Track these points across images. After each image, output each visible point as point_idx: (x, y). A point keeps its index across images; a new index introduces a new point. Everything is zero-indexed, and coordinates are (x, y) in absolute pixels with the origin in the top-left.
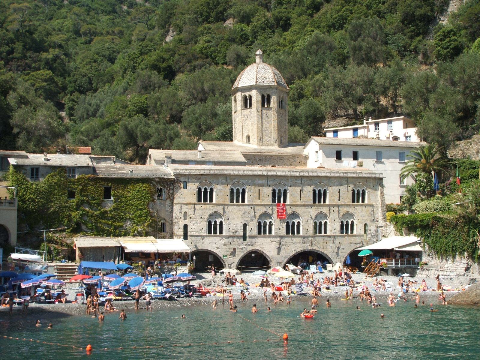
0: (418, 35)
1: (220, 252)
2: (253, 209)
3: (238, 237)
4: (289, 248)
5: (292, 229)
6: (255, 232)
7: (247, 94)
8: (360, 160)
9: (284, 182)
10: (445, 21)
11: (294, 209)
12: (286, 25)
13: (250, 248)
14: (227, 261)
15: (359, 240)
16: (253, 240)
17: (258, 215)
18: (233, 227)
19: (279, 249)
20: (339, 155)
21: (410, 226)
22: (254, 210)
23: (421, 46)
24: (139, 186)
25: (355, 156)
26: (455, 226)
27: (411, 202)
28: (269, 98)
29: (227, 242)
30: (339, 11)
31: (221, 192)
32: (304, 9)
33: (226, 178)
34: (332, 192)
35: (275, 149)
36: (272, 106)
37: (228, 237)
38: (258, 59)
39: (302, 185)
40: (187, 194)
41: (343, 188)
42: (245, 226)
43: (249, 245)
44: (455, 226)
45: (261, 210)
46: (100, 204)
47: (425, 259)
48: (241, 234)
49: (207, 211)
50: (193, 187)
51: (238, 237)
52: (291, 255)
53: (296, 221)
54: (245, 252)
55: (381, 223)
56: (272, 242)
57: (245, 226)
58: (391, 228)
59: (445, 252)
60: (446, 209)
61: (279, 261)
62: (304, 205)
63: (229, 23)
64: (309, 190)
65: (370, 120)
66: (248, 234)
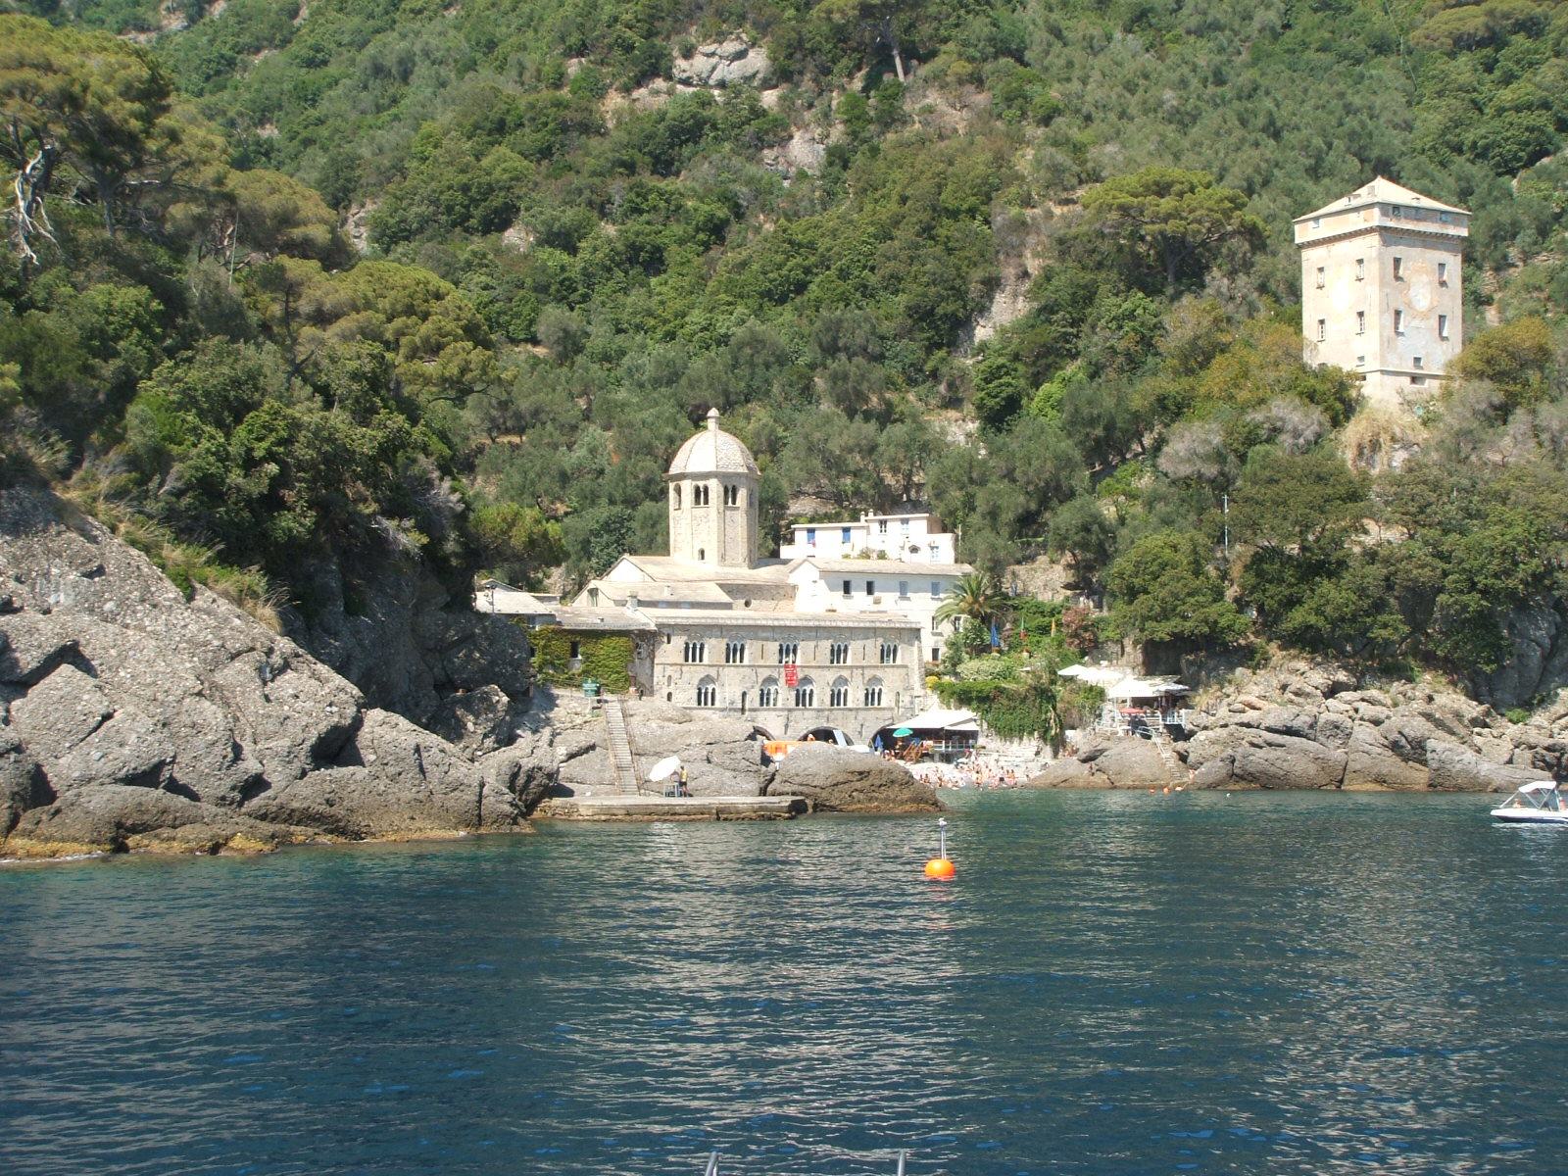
0: (939, 346)
5: (801, 699)
6: (757, 704)
7: (701, 484)
8: (877, 594)
10: (982, 332)
11: (807, 672)
12: (655, 262)
15: (888, 714)
20: (847, 588)
21: (964, 698)
23: (944, 370)
24: (615, 641)
25: (870, 589)
26: (1024, 700)
27: (955, 662)
28: (735, 491)
30: (780, 267)
31: (714, 649)
32: (690, 229)
33: (721, 630)
34: (855, 647)
35: (743, 573)
36: (739, 503)
38: (711, 424)
39: (817, 638)
40: (670, 652)
41: (869, 643)
42: (744, 694)
44: (1024, 700)
45: (765, 673)
46: (565, 666)
47: (981, 741)
50: (679, 642)
53: (808, 689)
55: (918, 690)
57: (744, 694)
58: (934, 699)
59: (1009, 731)
60: (1008, 673)
63: (515, 237)
64: (826, 645)
65: (871, 515)
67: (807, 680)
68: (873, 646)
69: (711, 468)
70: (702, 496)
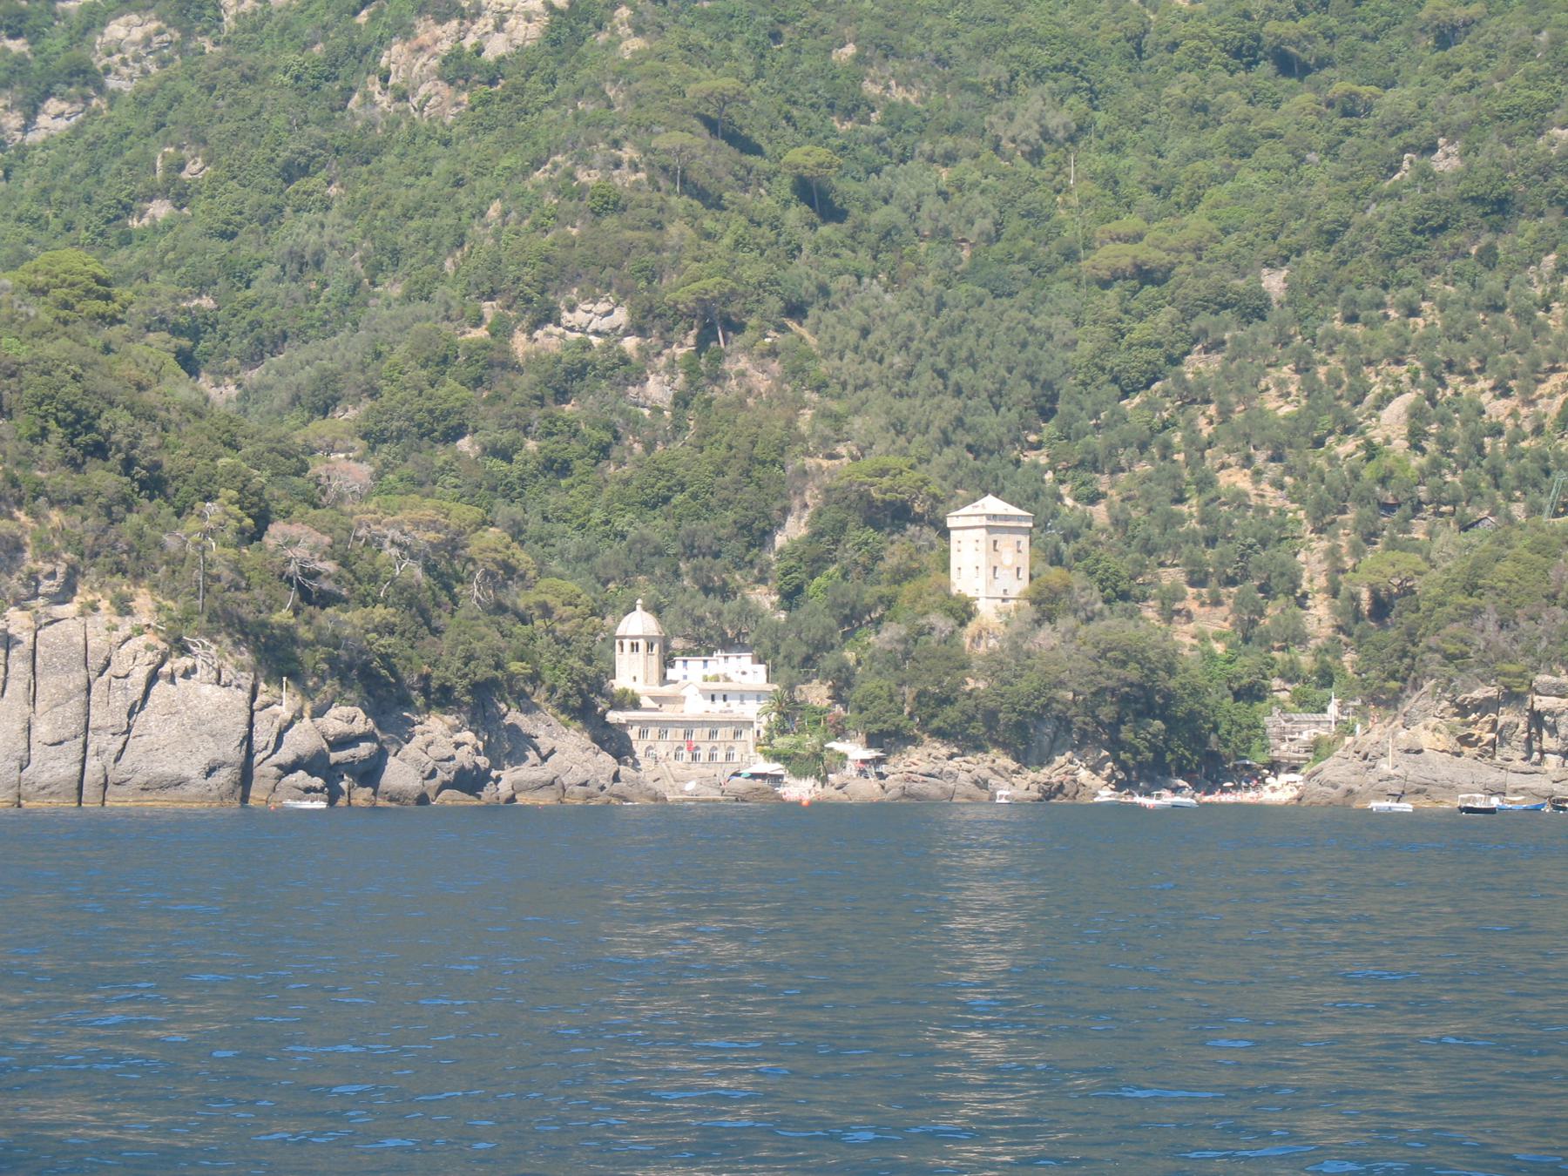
0: (754, 546)
10: (780, 540)
20: (713, 698)
21: (777, 757)
23: (757, 561)
25: (725, 698)
27: (771, 738)
34: (721, 731)
55: (752, 753)
58: (761, 758)
59: (800, 775)
60: (797, 746)
64: (707, 730)
67: (697, 748)
68: (730, 731)
69: (640, 633)
70: (635, 647)
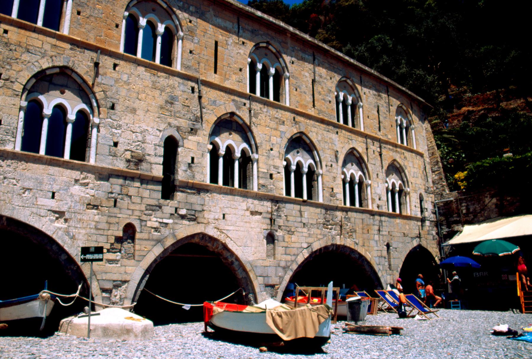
1: (71, 236)
2: (196, 95)
3: (145, 180)
4: (294, 238)
9: (277, 45)
13: (186, 230)
14: (98, 274)
16: (195, 199)
17: (210, 119)
18: (126, 140)
19: (271, 238)
22: (200, 97)
29: (101, 194)
37: (105, 175)
42: (171, 146)
43: (183, 217)
48: (158, 171)
49: (26, 57)
51: (145, 180)
52: (300, 259)
54: (169, 242)
56: (253, 213)
57: (171, 146)
61: (274, 280)
62: (322, 121)
66: (182, 174)
